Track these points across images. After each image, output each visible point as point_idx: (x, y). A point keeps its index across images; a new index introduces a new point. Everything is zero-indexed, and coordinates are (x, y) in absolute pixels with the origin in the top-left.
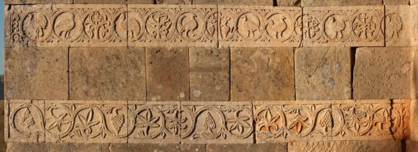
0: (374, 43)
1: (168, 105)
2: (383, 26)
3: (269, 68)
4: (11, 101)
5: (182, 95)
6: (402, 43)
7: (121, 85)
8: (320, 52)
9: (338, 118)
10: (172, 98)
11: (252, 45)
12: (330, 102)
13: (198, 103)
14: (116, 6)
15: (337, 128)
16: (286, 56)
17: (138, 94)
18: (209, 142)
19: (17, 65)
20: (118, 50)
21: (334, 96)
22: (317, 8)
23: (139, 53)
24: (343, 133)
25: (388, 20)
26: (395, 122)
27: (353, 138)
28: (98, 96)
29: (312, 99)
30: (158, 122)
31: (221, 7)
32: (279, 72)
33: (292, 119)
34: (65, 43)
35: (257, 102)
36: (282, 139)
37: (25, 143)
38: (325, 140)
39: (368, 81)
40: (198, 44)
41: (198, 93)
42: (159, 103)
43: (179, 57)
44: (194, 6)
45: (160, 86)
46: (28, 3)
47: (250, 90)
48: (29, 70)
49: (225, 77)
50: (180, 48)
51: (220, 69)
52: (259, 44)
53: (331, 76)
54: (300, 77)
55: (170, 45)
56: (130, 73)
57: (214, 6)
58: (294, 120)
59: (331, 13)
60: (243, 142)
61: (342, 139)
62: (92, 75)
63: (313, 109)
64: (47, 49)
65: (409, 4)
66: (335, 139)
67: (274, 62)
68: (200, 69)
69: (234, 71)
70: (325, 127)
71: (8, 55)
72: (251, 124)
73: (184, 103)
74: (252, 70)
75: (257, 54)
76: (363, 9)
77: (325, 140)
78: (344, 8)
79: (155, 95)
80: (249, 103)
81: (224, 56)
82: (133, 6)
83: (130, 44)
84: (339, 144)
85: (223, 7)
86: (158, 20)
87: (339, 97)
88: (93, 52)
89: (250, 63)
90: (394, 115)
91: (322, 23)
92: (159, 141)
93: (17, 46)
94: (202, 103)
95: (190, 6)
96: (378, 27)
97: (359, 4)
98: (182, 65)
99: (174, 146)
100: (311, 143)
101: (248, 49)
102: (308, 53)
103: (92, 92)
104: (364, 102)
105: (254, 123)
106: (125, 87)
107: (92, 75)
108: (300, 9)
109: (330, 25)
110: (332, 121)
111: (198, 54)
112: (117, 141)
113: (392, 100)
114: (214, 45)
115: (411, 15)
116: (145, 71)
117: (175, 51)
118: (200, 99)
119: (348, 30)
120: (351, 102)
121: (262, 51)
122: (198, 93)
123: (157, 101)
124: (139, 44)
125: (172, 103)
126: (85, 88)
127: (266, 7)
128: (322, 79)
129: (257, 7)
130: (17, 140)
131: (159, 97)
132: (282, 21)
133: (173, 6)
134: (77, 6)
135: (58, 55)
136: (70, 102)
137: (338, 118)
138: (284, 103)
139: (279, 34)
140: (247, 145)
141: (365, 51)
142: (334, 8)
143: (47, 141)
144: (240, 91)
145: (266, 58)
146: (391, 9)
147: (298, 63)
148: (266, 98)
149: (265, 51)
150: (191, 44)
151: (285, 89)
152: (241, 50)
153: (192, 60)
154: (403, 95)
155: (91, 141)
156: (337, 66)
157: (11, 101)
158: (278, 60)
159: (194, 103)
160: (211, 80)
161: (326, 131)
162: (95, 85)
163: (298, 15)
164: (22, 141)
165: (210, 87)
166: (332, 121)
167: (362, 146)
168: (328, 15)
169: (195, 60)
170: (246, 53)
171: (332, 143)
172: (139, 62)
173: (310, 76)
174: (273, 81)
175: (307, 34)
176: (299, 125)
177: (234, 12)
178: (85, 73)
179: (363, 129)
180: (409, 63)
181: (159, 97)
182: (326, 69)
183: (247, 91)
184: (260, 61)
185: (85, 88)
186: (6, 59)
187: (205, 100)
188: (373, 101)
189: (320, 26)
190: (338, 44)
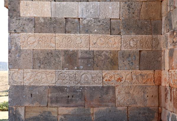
0: (148, 49)
1: (71, 72)
2: (151, 42)
3: (108, 58)
4: (11, 69)
5: (76, 68)
6: (159, 49)
7: (53, 64)
8: (127, 52)
9: (134, 77)
10: (72, 69)
11: (102, 49)
13: (82, 71)
14: (51, 34)
15: (134, 81)
16: (115, 53)
17: (59, 67)
18: (86, 86)
19: (13, 56)
20: (52, 51)
22: (127, 36)
23: (59, 51)
25: (153, 41)
27: (140, 85)
28: (44, 68)
29: (125, 70)
30: (67, 78)
31: (91, 35)
32: (112, 60)
33: (117, 77)
34: (32, 48)
35: (104, 71)
36: (113, 85)
37: (16, 86)
38: (129, 85)
39: (146, 63)
40: (82, 49)
41: (82, 67)
42: (67, 71)
43: (75, 53)
44: (80, 34)
45: (67, 64)
46: (18, 32)
47: (102, 66)
48: (17, 58)
49: (92, 61)
50: (75, 50)
51: (90, 58)
52: (104, 49)
53: (131, 61)
54: (120, 62)
55: (71, 49)
56: (57, 59)
57: (88, 35)
58: (118, 78)
59: (132, 38)
60: (99, 85)
62: (42, 60)
63: (125, 73)
64: (25, 50)
65: (161, 34)
67: (110, 56)
68: (82, 58)
69: (95, 59)
71: (9, 52)
72: (102, 79)
73: (77, 71)
74: (102, 59)
75: (104, 53)
76: (144, 36)
77: (129, 85)
78: (137, 36)
79: (65, 68)
80: (101, 71)
81: (92, 53)
82: (57, 34)
83: (57, 49)
85: (91, 35)
86: (66, 39)
87: (135, 69)
88: (42, 51)
89: (101, 56)
90: (155, 76)
91: (128, 41)
92: (67, 85)
93: (13, 49)
94: (83, 71)
95: (79, 34)
96: (150, 43)
97: (143, 34)
98: (76, 56)
99: (72, 87)
100: (124, 86)
101: (101, 51)
102: (123, 53)
103: (42, 66)
104: (144, 71)
105: (103, 78)
106: (54, 65)
107: (42, 60)
108: (120, 36)
109: (131, 42)
111: (82, 53)
112: (51, 85)
113: (154, 70)
114: (88, 49)
115: (162, 38)
116: (62, 58)
117: (73, 51)
118: (83, 69)
119: (138, 44)
120: (139, 71)
121: (106, 52)
122: (82, 67)
123: (67, 70)
124: (60, 49)
125: (72, 71)
126: (39, 65)
127: (108, 35)
128: (128, 62)
129: (104, 35)
130: (13, 84)
131: (67, 69)
132: (113, 40)
133: (73, 34)
134: (36, 34)
135: (29, 52)
136: (33, 70)
137: (134, 77)
138: (114, 71)
139: (112, 45)
140: (100, 87)
141: (145, 52)
142: (133, 35)
143: (25, 85)
144: (97, 67)
145: (107, 54)
146: (154, 36)
147: (119, 56)
148: (107, 69)
149: (107, 52)
150: (79, 49)
151: (114, 66)
152: (98, 51)
153: (80, 55)
155: (41, 85)
156: (134, 57)
157: (11, 69)
158: (112, 55)
159: (80, 71)
160: (87, 62)
162: (43, 64)
163: (120, 38)
164: (15, 85)
165: (86, 65)
167: (143, 88)
168: (131, 38)
169: (81, 55)
170: (100, 53)
172: (60, 55)
173: (124, 61)
174: (110, 63)
175: (123, 45)
176: (120, 79)
177: (95, 37)
178: (39, 59)
179: (144, 81)
180: (161, 57)
181: (67, 69)
182: (130, 59)
183: (100, 66)
184: (105, 55)
185: (39, 65)
186: (9, 53)
187: (85, 70)
188: (149, 71)
189: (128, 43)
190: (134, 49)
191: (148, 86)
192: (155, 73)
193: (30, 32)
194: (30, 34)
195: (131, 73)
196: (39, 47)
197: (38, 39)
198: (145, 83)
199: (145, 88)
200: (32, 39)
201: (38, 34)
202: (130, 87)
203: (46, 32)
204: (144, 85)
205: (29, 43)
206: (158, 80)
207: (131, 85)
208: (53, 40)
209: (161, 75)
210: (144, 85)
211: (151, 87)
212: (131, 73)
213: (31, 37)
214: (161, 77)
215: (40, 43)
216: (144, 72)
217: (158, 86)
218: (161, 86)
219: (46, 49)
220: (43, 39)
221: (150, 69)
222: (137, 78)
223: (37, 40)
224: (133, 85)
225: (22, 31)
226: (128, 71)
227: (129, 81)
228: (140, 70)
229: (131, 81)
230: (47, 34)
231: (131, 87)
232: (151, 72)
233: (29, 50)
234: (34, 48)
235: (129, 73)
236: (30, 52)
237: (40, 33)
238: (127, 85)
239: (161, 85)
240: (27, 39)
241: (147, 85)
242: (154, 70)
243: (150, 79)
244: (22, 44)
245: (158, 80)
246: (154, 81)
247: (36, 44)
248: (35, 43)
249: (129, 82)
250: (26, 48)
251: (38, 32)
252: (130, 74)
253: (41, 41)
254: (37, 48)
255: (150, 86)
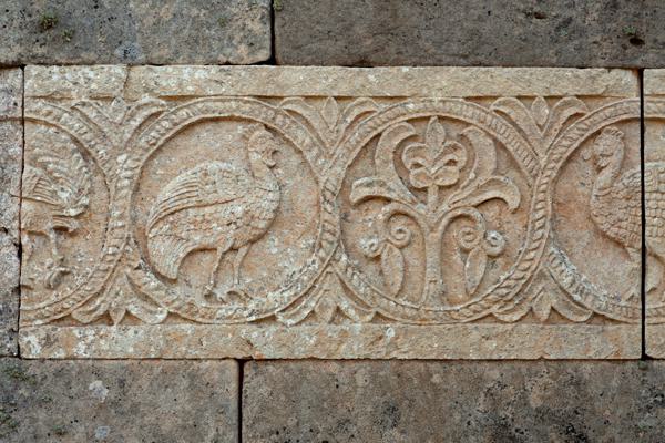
14: (568, 81)
20: (578, 383)
134: (294, 78)
193: (194, 48)
194: (189, 76)
196: (358, 324)
197: (331, 175)
200: (218, 179)
201: (330, 78)
203: (475, 54)
205: (167, 253)
208: (607, 195)
213: (204, 133)
215: (365, 244)
219: (474, 343)
220: (431, 166)
223: (305, 198)
225: (47, 25)
230: (501, 80)
233: (165, 381)
234: (266, 342)
236: (184, 402)
237: (363, 62)
240: (125, 166)
244: (40, 270)
247: (290, 257)
248: (272, 246)
250: (122, 342)
251: (331, 47)
253: (380, 212)
254: (306, 341)
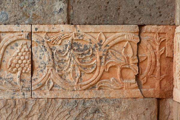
12: (28, 28)
15: (40, 77)
21: (35, 17)
24: (52, 84)
26: (147, 67)
27: (69, 94)
38: (19, 96)
61: (48, 95)
66: (36, 94)
70: (18, 73)
77: (19, 96)
84: (43, 103)
87: (45, 18)
90: (144, 54)
104: (91, 28)
110: (32, 62)
113: (141, 26)
120: (66, 29)
137: (42, 57)
154: (161, 19)
161: (21, 80)
166: (32, 62)
167: (86, 109)
171: (31, 102)
179: (89, 79)
191: (106, 100)
192: (145, 38)
195: (30, 35)
198: (93, 87)
199: (96, 111)
202: (20, 107)
204: (87, 94)
206: (157, 74)
207: (28, 95)
209: (172, 46)
210: (87, 94)
211: (125, 105)
212: (30, 35)
214: (171, 59)
216: (91, 33)
217: (159, 100)
218: (169, 101)
221: (121, 19)
222: (56, 63)
224: (36, 94)
226: (14, 28)
227: (16, 77)
228: (69, 22)
229: (28, 77)
231: (26, 105)
232: (125, 32)
235: (16, 36)
238: (7, 97)
239: (169, 94)
241: (102, 94)
242: (141, 26)
243: (118, 70)
245: (157, 74)
246: (137, 77)
249: (18, 80)
252: (20, 43)
255: (117, 103)
